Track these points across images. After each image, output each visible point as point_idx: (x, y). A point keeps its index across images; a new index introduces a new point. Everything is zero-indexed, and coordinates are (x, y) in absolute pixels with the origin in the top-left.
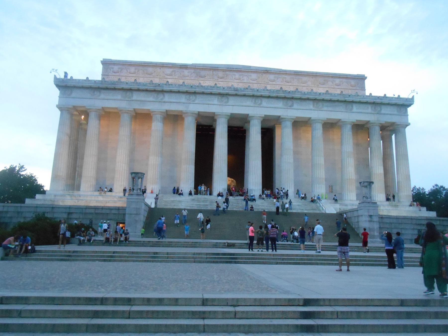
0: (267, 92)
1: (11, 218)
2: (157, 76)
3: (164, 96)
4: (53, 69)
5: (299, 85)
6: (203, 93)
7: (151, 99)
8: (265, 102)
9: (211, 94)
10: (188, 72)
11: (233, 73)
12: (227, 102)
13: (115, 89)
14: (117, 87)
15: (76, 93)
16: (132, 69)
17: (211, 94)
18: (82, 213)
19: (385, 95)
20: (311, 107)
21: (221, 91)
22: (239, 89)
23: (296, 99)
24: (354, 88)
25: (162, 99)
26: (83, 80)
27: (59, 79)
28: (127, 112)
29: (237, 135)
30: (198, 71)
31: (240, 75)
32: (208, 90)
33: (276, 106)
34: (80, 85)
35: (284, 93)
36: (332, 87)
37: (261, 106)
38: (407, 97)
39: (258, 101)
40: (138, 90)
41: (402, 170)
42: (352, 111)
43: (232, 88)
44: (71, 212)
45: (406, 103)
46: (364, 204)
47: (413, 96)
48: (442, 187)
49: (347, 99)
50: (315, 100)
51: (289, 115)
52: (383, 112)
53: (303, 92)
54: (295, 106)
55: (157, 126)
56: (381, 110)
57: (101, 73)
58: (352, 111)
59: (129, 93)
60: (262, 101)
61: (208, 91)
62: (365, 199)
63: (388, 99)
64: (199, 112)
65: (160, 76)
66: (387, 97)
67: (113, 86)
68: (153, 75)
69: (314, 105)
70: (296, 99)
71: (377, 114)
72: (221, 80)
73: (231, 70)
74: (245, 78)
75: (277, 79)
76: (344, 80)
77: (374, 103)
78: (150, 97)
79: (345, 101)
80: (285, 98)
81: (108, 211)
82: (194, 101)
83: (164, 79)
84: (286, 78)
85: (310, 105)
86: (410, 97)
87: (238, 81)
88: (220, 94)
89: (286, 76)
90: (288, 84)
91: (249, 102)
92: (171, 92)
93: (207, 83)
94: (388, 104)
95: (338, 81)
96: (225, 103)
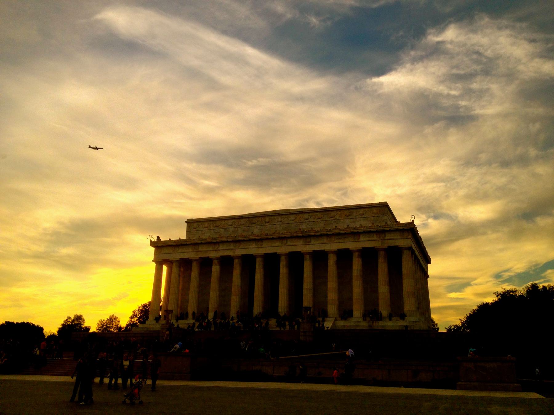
6: (244, 241)
7: (211, 249)
8: (289, 243)
12: (262, 245)
15: (166, 250)
20: (325, 241)
28: (196, 260)
34: (166, 244)
39: (284, 241)
40: (201, 243)
47: (413, 221)
52: (387, 238)
54: (313, 242)
74: (286, 220)
76: (367, 209)
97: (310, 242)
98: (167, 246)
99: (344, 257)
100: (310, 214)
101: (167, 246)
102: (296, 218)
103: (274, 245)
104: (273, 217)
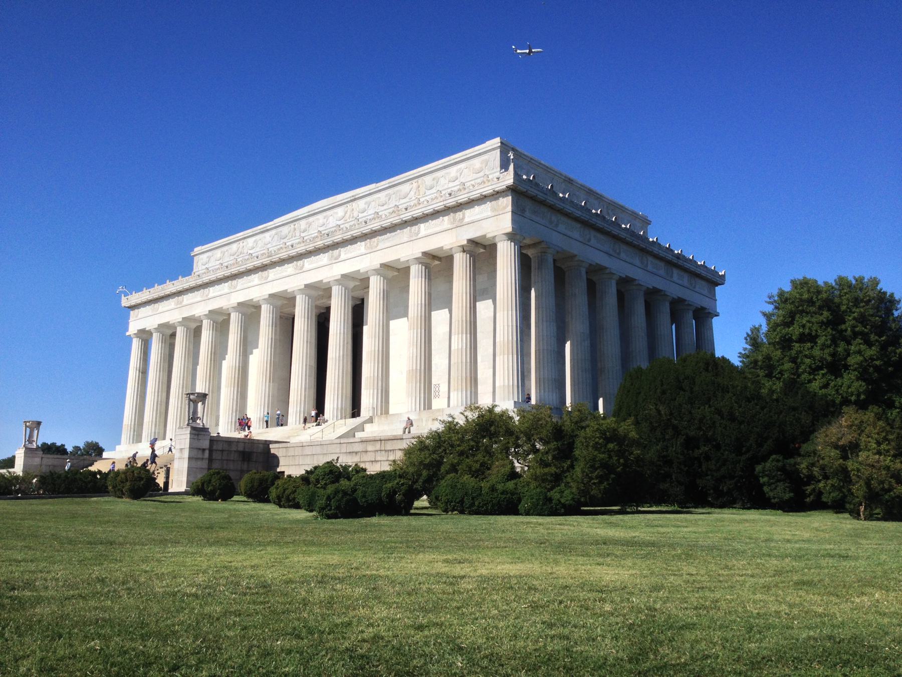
36: (446, 187)
50: (364, 237)
52: (467, 220)
54: (343, 257)
55: (206, 336)
63: (467, 191)
75: (369, 204)
76: (462, 166)
79: (404, 224)
82: (235, 288)
100: (368, 199)
103: (285, 274)
104: (311, 219)
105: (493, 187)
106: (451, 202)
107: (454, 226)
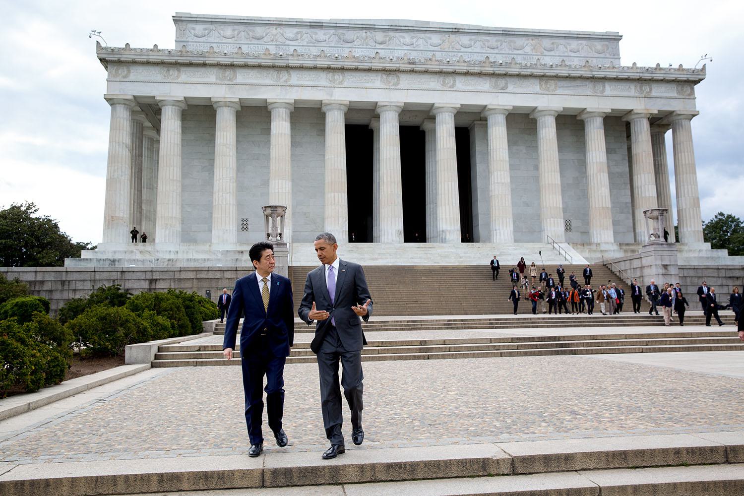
0: (463, 64)
1: (51, 291)
2: (272, 41)
3: (290, 74)
4: (95, 31)
5: (510, 52)
6: (357, 69)
8: (460, 83)
9: (370, 70)
10: (324, 34)
11: (401, 34)
12: (398, 84)
13: (204, 65)
14: (209, 61)
15: (138, 73)
16: (228, 31)
17: (370, 70)
18: (175, 280)
19: (658, 65)
21: (388, 66)
22: (417, 61)
23: (511, 76)
24: (602, 55)
25: (286, 81)
26: (148, 50)
27: (106, 48)
28: (228, 104)
29: (415, 141)
30: (341, 31)
31: (412, 38)
32: (366, 64)
33: (479, 88)
34: (144, 58)
35: (491, 67)
36: (566, 54)
37: (455, 89)
38: (693, 67)
39: (449, 80)
40: (246, 66)
41: (686, 191)
42: (606, 93)
43: (406, 58)
44: (154, 278)
45: (692, 78)
46: (654, 246)
48: (729, 216)
49: (597, 74)
50: (542, 77)
51: (500, 104)
52: (654, 94)
53: (523, 64)
54: (511, 88)
55: (281, 126)
56: (651, 89)
57: (174, 38)
58: (606, 93)
59: (229, 73)
60: (455, 81)
61: (366, 65)
62: (653, 238)
63: (662, 72)
64: (350, 102)
65: (276, 41)
66: (661, 69)
67: (202, 59)
68: (265, 39)
69: (541, 86)
70: (511, 76)
71: (645, 97)
72: (382, 46)
73: (397, 29)
74: (421, 42)
76: (584, 42)
77: (640, 80)
78: (268, 78)
79: (593, 79)
80: (493, 75)
81: (218, 275)
82: (341, 83)
83: (284, 47)
84: (488, 41)
85: (534, 86)
86: (700, 67)
87: (408, 48)
88: (384, 71)
89: (488, 38)
90: (492, 51)
91: (434, 82)
92: (301, 68)
93: (361, 50)
94: (663, 81)
95: (574, 44)
96: (394, 85)
97: (507, 88)
98: (148, 63)
99: (571, 124)
100: (473, 37)
101: (148, 63)
102: (444, 41)
103: (425, 87)
104: (391, 34)
105: (688, 76)
106: (647, 76)
107: (643, 96)
